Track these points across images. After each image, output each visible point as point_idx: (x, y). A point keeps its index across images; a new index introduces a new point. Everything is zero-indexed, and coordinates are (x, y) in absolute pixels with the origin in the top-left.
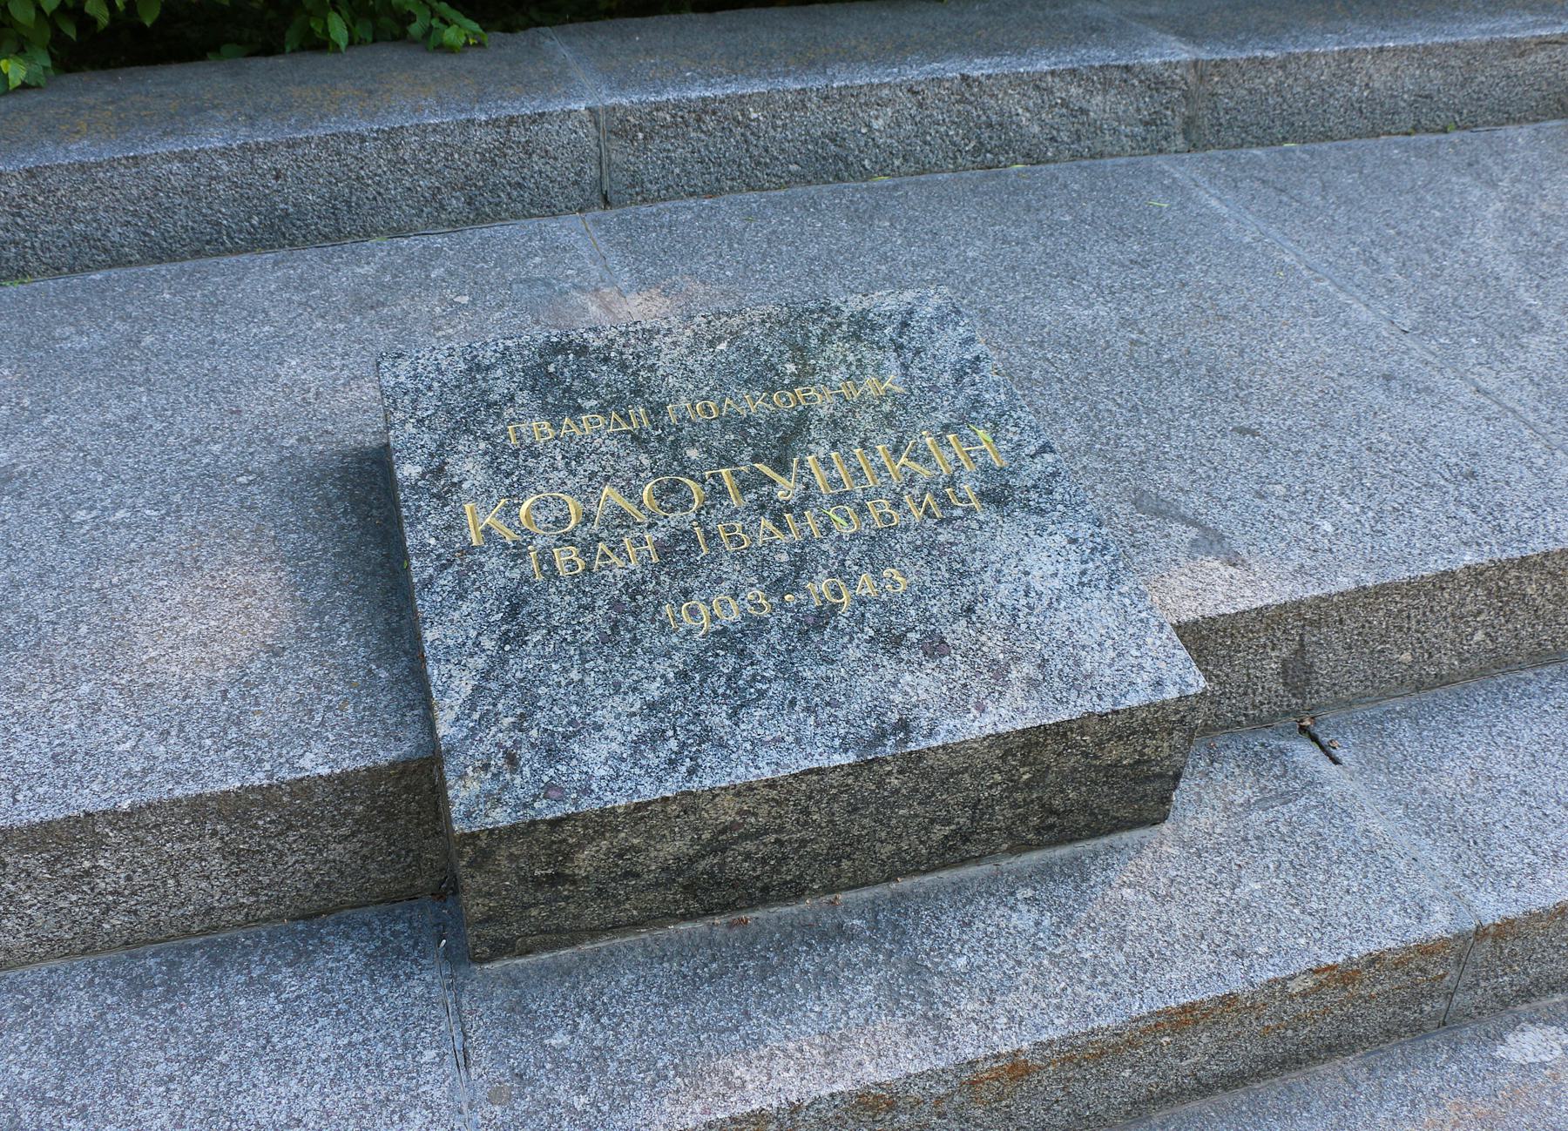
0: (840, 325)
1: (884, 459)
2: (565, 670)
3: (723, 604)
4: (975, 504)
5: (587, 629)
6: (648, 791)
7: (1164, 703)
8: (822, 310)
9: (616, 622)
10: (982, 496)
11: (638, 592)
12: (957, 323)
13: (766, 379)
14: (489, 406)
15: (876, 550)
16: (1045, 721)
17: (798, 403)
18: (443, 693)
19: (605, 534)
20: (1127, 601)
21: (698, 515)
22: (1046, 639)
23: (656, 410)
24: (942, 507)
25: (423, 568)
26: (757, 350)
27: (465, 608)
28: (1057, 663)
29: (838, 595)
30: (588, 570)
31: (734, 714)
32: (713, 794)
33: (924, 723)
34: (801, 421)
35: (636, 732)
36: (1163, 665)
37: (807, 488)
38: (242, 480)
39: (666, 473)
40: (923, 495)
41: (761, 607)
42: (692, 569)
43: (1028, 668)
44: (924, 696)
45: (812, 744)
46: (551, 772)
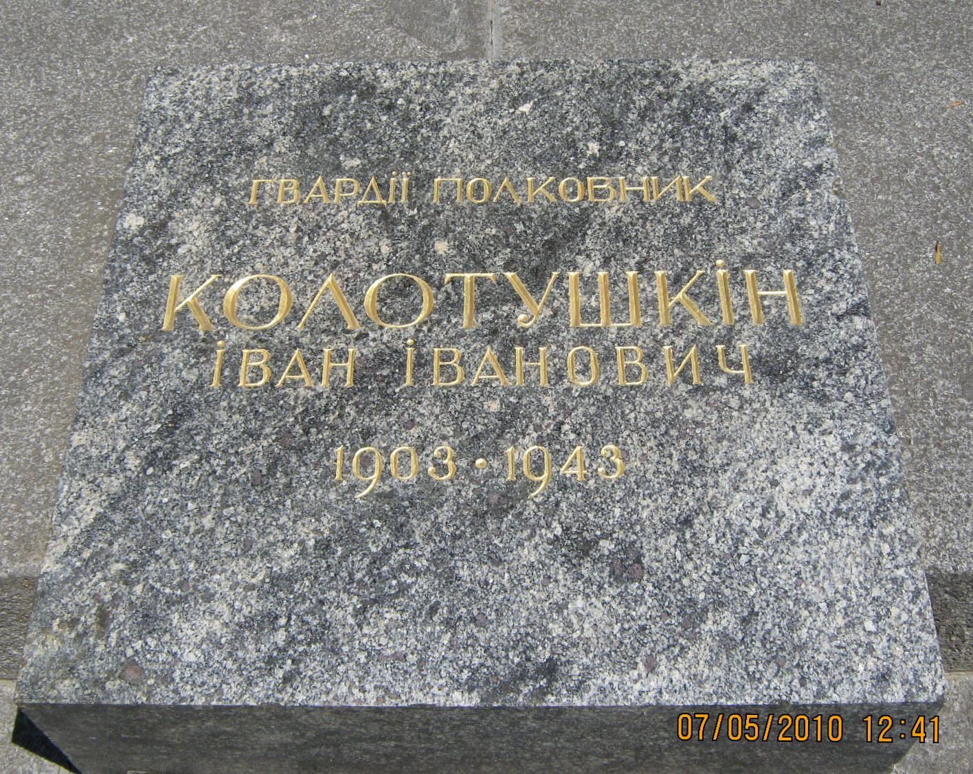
0: (670, 98)
1: (659, 291)
2: (201, 513)
4: (744, 372)
5: (242, 463)
6: (232, 694)
7: (882, 706)
8: (658, 75)
10: (758, 363)
12: (811, 116)
13: (559, 158)
14: (242, 151)
15: (606, 412)
16: (723, 701)
17: (585, 198)
18: (64, 517)
19: (304, 340)
20: (886, 548)
21: (418, 331)
22: (766, 581)
24: (706, 370)
25: (101, 350)
26: (563, 117)
27: (126, 409)
28: (767, 620)
29: (538, 470)
31: (360, 612)
33: (576, 671)
34: (582, 220)
35: (246, 611)
36: (898, 651)
37: (555, 315)
38: (19, 179)
39: (402, 270)
40: (687, 348)
43: (728, 620)
44: (589, 632)
45: (436, 671)
46: (138, 645)
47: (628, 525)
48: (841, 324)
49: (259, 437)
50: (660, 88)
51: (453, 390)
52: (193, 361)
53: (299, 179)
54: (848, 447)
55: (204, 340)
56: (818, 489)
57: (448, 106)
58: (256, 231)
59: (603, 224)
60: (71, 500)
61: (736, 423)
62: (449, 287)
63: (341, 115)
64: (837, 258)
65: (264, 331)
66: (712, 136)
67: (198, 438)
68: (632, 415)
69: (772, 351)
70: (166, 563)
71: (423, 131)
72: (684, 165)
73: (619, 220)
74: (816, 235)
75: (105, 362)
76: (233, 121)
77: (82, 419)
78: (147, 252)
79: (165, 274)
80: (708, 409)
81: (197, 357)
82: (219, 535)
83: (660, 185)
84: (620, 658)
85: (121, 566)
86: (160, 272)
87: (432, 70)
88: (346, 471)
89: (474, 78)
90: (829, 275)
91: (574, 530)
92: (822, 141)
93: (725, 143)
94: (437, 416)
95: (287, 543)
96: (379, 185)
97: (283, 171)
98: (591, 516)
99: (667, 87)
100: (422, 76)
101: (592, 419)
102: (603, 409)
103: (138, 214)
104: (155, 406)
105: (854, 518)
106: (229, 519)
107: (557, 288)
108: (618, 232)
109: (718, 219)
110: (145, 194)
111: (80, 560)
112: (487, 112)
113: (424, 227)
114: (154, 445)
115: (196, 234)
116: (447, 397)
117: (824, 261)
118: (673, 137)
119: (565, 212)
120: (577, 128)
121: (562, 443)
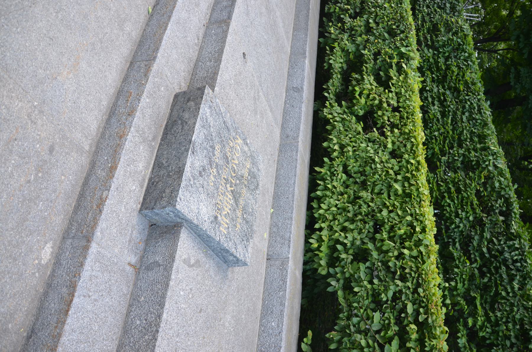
32: (196, 120)
84: (192, 164)
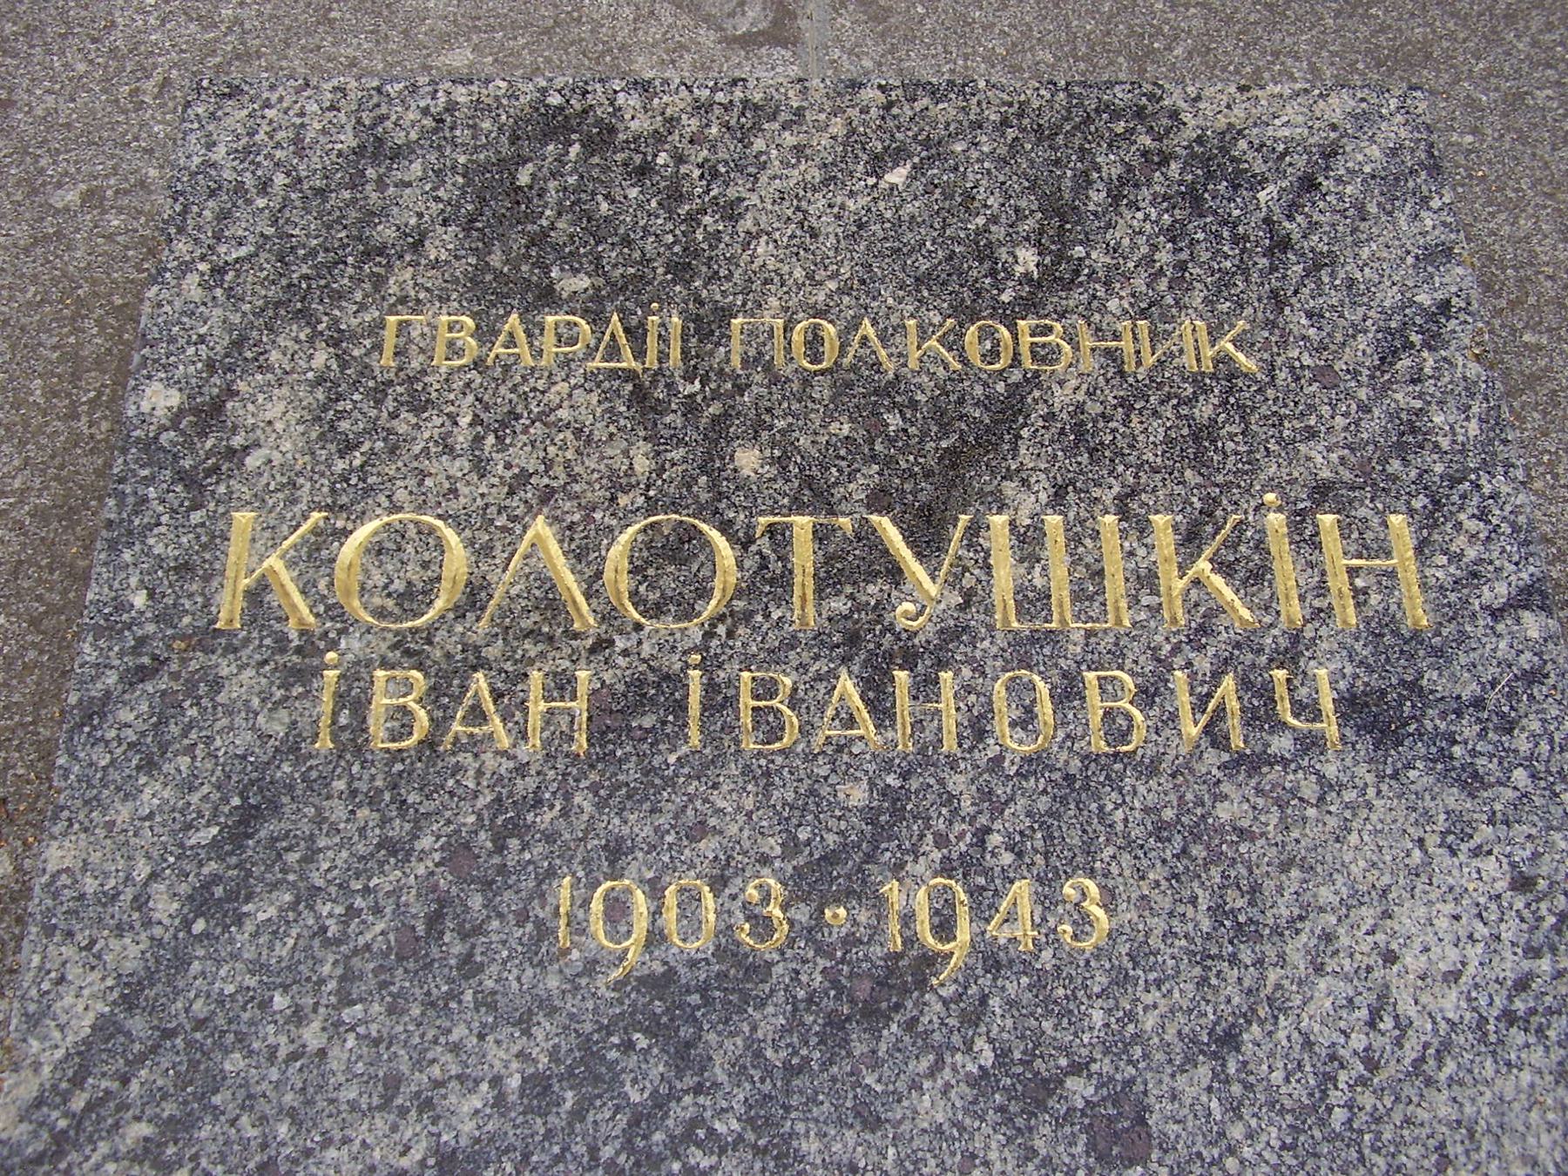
0: (1165, 160)
2: (298, 1016)
3: (690, 899)
4: (1330, 728)
5: (377, 910)
9: (443, 902)
10: (1350, 705)
11: (516, 828)
12: (1425, 201)
13: (964, 285)
14: (367, 255)
17: (1016, 360)
18: (33, 1022)
19: (492, 652)
21: (709, 635)
23: (707, 326)
24: (1252, 719)
25: (101, 667)
27: (152, 793)
29: (944, 929)
30: (430, 743)
34: (1010, 410)
37: (964, 607)
39: (674, 506)
40: (1217, 676)
41: (763, 926)
42: (645, 794)
47: (1118, 1045)
48: (1500, 627)
49: (409, 853)
50: (1146, 141)
51: (779, 760)
52: (279, 694)
53: (474, 315)
54: (1522, 883)
55: (299, 650)
56: (1471, 970)
57: (752, 170)
58: (395, 423)
59: (1050, 417)
60: (45, 986)
61: (1313, 831)
62: (764, 544)
63: (552, 184)
64: (1487, 490)
65: (414, 631)
66: (1245, 238)
67: (292, 857)
68: (1119, 815)
69: (1375, 681)
70: (233, 1122)
71: (707, 220)
72: (1197, 298)
73: (1080, 408)
74: (1445, 443)
75: (108, 694)
76: (347, 195)
77: (66, 813)
78: (187, 463)
79: (221, 510)
80: (1261, 802)
81: (286, 686)
82: (334, 1065)
83: (1154, 336)
85: (144, 1129)
86: (212, 506)
87: (720, 97)
88: (579, 928)
89: (799, 112)
90: (1472, 525)
91: (1017, 1055)
92: (1447, 252)
93: (1268, 253)
94: (749, 815)
95: (468, 1082)
96: (627, 330)
97: (444, 300)
98: (1047, 1025)
99: (1159, 139)
100: (701, 108)
101: (1045, 823)
102: (1064, 801)
103: (169, 382)
104: (205, 789)
105: (1540, 1031)
106: (352, 1029)
107: (969, 547)
108: (1078, 433)
109: (1264, 410)
110: (182, 342)
111: (65, 1115)
112: (825, 182)
113: (715, 420)
114: (205, 870)
115: (279, 426)
116: (767, 774)
117: (1463, 497)
118: (1173, 240)
119: (978, 390)
120: (994, 220)
121: (986, 872)
